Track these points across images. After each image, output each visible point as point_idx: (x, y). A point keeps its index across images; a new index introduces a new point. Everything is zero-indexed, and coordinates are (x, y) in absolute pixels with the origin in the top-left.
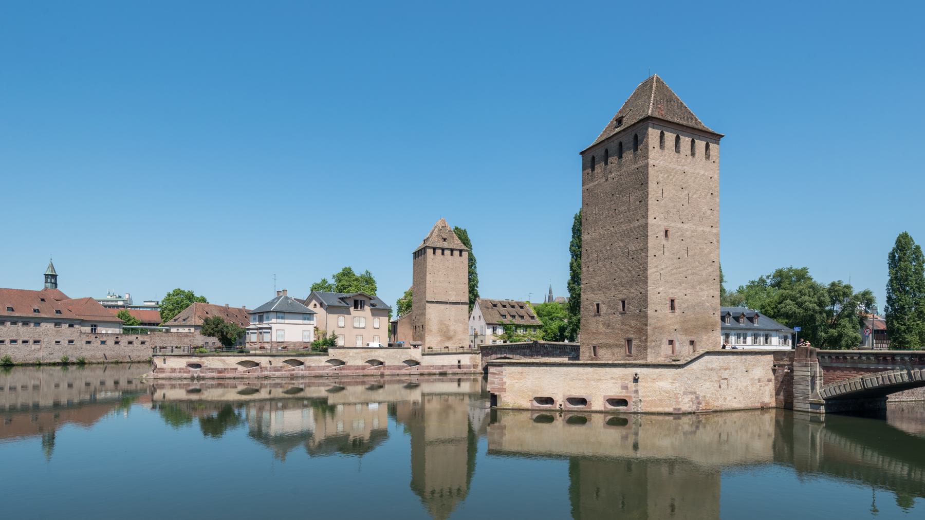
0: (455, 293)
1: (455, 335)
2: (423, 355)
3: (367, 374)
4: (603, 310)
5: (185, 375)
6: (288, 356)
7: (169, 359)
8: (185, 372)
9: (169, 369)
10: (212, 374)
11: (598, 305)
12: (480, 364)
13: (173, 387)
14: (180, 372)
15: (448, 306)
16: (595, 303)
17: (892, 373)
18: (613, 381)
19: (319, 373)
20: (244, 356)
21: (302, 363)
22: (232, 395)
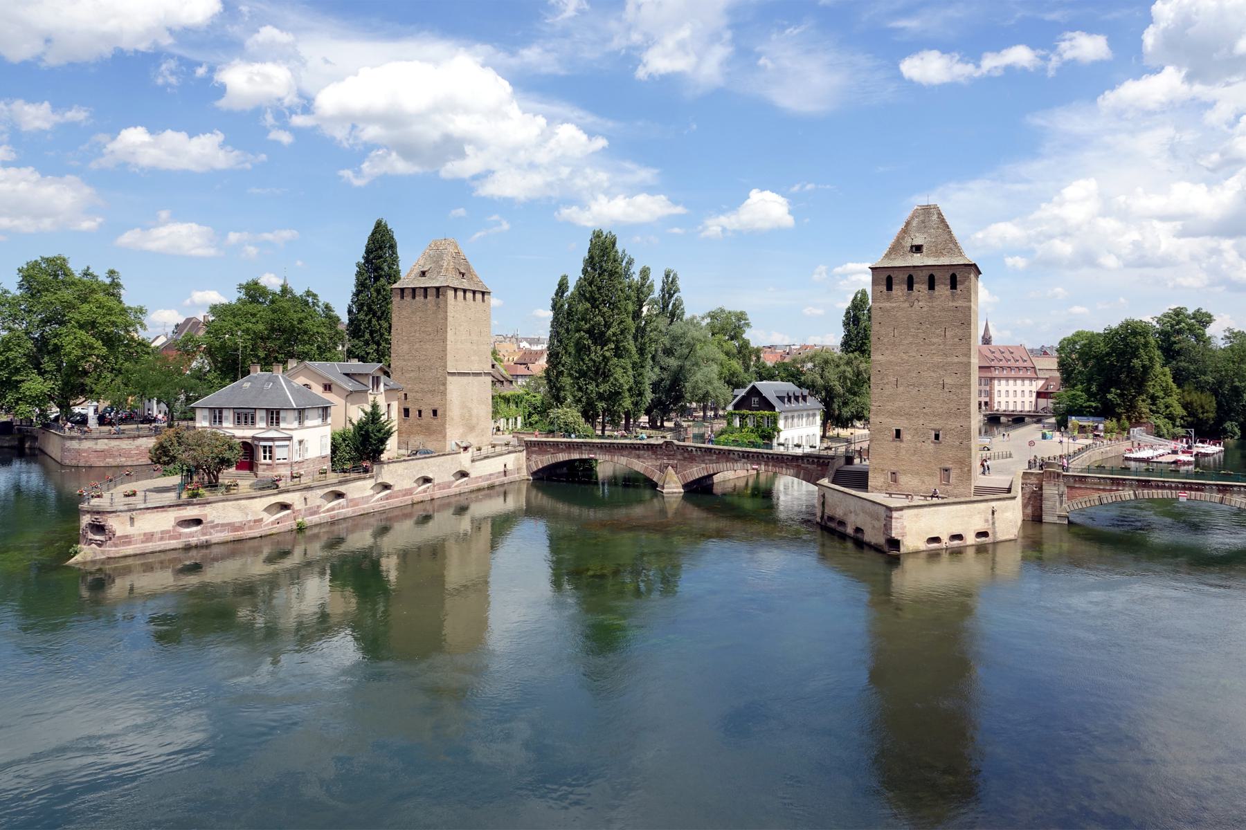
0: (477, 358)
1: (478, 424)
2: (473, 461)
3: (416, 500)
4: (906, 436)
5: (174, 543)
6: (327, 485)
7: (140, 517)
8: (171, 538)
9: (140, 535)
10: (222, 534)
11: (898, 433)
12: (525, 467)
13: (149, 568)
14: (162, 539)
15: (471, 378)
16: (894, 428)
17: (1122, 493)
18: (979, 516)
19: (364, 509)
20: (274, 494)
21: (339, 495)
22: (257, 568)
